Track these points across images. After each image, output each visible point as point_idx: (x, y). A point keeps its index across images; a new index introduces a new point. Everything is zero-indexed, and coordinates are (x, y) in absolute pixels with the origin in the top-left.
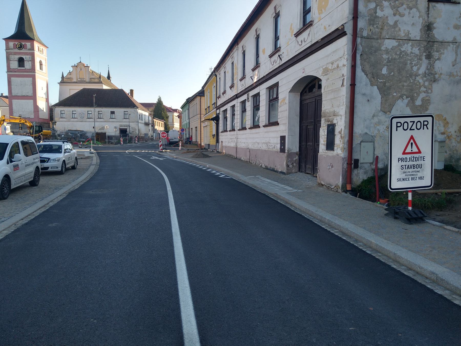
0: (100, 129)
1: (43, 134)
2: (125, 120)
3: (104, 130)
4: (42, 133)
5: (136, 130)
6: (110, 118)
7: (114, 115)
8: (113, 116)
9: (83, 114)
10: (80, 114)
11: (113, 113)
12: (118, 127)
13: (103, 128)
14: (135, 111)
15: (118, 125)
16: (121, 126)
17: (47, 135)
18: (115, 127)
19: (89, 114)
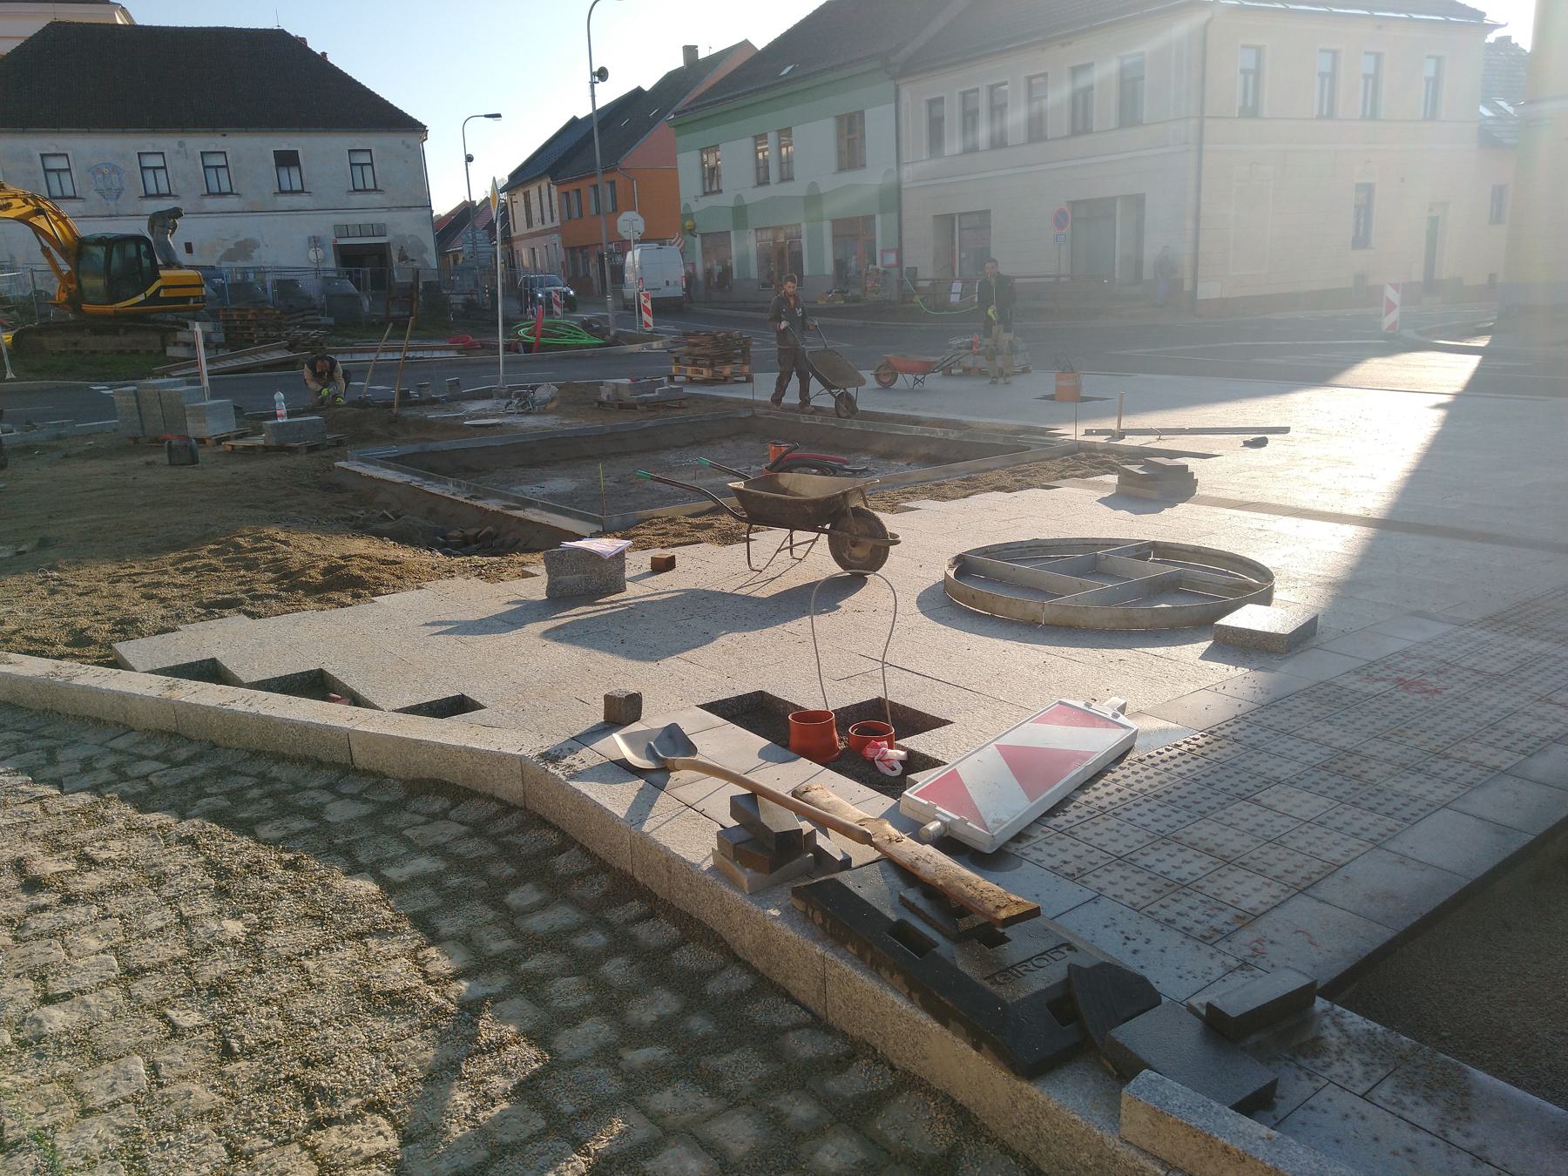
0: (229, 256)
1: (162, 294)
2: (358, 199)
3: (248, 257)
4: (158, 291)
5: (424, 249)
6: (277, 190)
7: (294, 172)
8: (292, 178)
9: (114, 169)
10: (95, 170)
11: (287, 160)
12: (330, 237)
13: (245, 248)
14: (408, 147)
15: (323, 226)
16: (342, 230)
17: (185, 300)
18: (315, 242)
19: (149, 175)
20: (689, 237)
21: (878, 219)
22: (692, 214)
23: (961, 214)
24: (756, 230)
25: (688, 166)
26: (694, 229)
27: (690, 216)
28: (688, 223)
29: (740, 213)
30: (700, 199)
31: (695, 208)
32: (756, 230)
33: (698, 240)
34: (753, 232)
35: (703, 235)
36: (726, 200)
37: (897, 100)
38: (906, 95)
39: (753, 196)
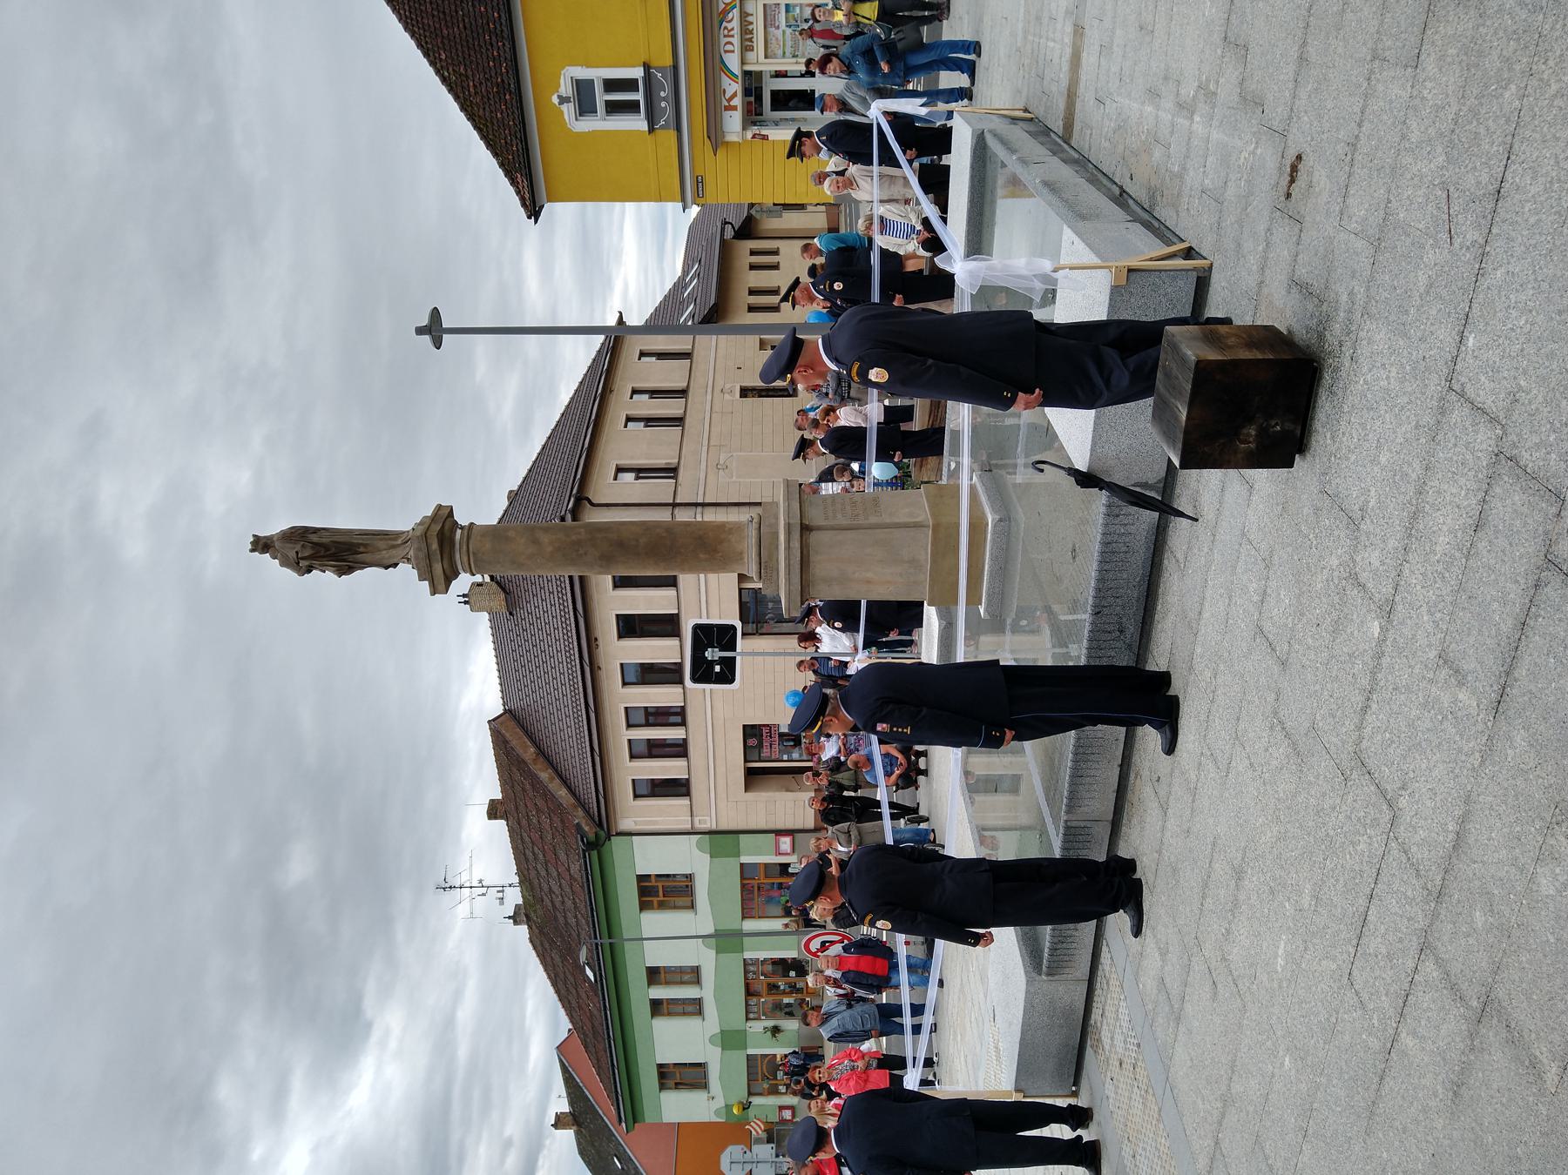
20: (751, 1112)
21: (745, 859)
22: (726, 1106)
23: (746, 761)
24: (748, 1019)
25: (678, 1107)
26: (743, 1103)
27: (728, 1107)
28: (735, 1111)
29: (730, 1040)
30: (711, 1095)
31: (720, 1103)
32: (748, 1019)
33: (756, 1100)
34: (750, 1024)
35: (750, 1094)
36: (712, 1056)
37: (631, 834)
38: (625, 824)
39: (711, 1022)
